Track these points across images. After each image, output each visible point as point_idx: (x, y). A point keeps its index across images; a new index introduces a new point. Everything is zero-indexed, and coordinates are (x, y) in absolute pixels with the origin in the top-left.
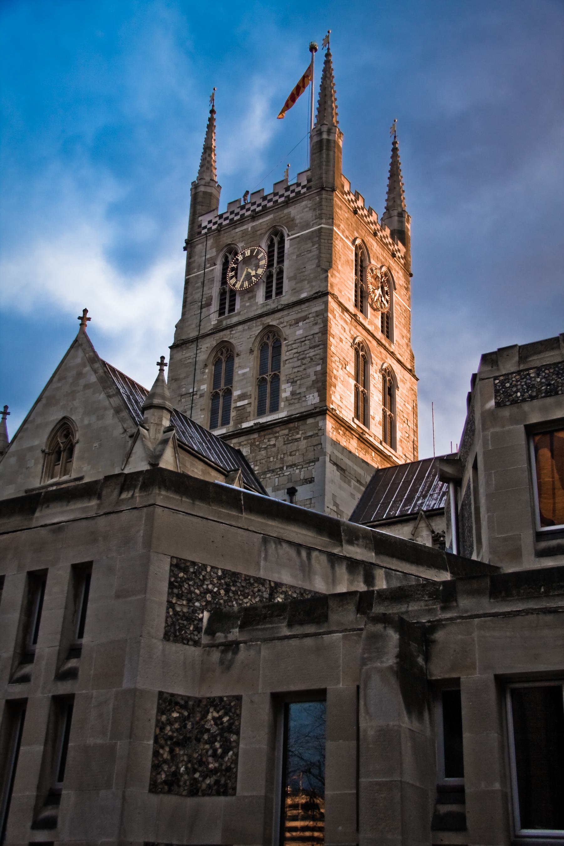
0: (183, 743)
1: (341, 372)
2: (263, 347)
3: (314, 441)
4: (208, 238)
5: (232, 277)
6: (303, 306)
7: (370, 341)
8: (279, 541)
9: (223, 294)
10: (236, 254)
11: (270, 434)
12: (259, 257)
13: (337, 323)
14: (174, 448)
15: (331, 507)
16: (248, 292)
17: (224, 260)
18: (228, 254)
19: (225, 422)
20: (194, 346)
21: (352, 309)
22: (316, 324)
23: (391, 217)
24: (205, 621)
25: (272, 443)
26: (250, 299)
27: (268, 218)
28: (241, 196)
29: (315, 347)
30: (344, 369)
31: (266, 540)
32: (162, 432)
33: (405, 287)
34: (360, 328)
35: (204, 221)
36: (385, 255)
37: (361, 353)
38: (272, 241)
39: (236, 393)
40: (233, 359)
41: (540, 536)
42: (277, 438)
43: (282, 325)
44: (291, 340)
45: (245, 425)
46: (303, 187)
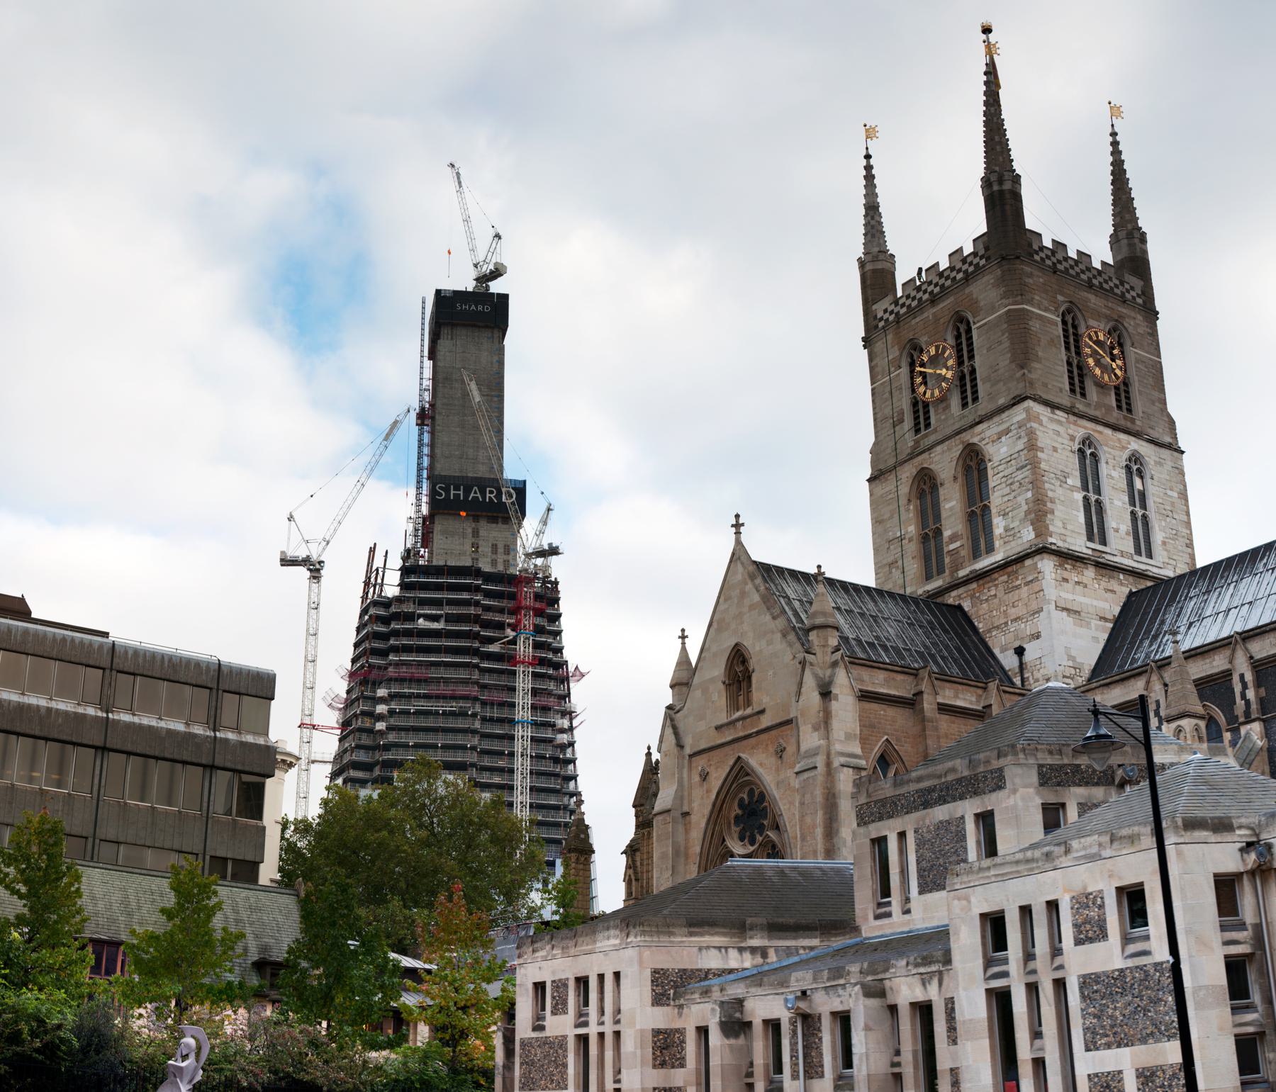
0: (667, 1048)
1: (1060, 491)
2: (967, 470)
3: (1035, 586)
4: (887, 332)
6: (1004, 415)
7: (1100, 433)
9: (915, 403)
10: (921, 351)
11: (989, 582)
12: (946, 355)
13: (1045, 430)
15: (1065, 663)
16: (942, 401)
17: (909, 360)
18: (912, 352)
19: (941, 571)
20: (892, 477)
21: (1065, 400)
22: (1020, 438)
24: (672, 995)
25: (993, 593)
27: (948, 301)
28: (915, 274)
29: (1022, 467)
30: (1065, 485)
31: (700, 949)
32: (830, 653)
33: (1148, 333)
35: (879, 308)
36: (1110, 304)
37: (1088, 452)
38: (958, 329)
39: (947, 533)
42: (996, 586)
43: (984, 442)
44: (996, 459)
45: (962, 573)
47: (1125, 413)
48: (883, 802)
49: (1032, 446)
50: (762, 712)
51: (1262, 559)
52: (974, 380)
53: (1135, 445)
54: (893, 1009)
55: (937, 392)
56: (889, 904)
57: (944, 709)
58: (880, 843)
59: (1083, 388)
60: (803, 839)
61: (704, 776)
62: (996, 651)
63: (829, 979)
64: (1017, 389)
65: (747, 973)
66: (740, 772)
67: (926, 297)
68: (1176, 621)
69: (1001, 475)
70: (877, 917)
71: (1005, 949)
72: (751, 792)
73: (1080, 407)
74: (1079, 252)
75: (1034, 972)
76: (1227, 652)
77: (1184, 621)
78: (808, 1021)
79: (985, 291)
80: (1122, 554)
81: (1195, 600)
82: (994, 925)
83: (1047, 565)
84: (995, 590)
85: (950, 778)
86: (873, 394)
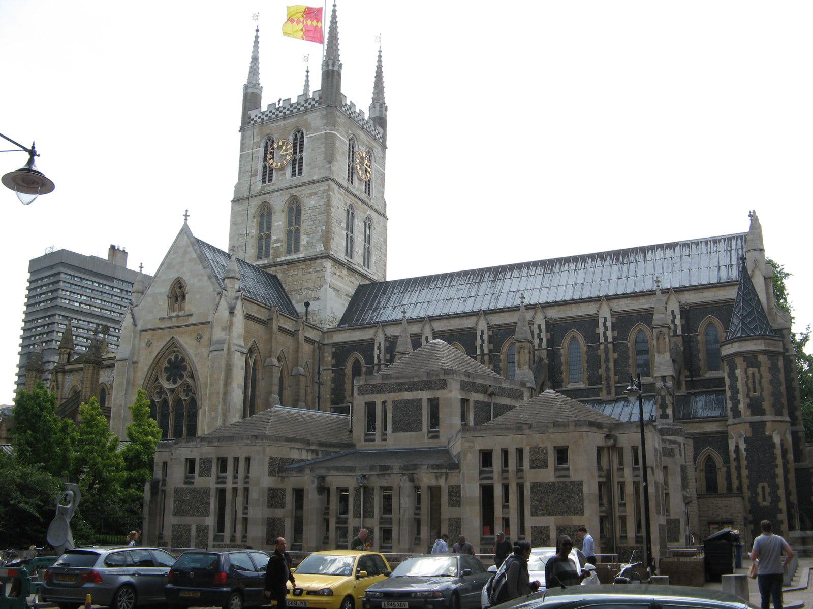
1: (337, 228)
2: (290, 209)
3: (321, 274)
5: (270, 159)
7: (357, 203)
8: (294, 448)
9: (265, 167)
10: (273, 142)
14: (242, 300)
19: (267, 256)
21: (345, 183)
22: (322, 198)
23: (374, 107)
26: (282, 174)
29: (322, 213)
31: (291, 448)
34: (350, 196)
35: (252, 113)
38: (296, 135)
39: (274, 238)
40: (271, 214)
41: (366, 435)
42: (298, 270)
44: (308, 206)
45: (279, 259)
46: (316, 102)
47: (367, 195)
48: (374, 386)
49: (328, 204)
50: (191, 315)
51: (433, 282)
52: (301, 163)
53: (370, 212)
54: (417, 488)
55: (279, 165)
56: (373, 435)
57: (281, 329)
58: (371, 407)
59: (352, 179)
60: (211, 385)
61: (149, 344)
62: (294, 302)
63: (380, 471)
64: (325, 174)
65: (310, 462)
66: (173, 345)
67: (281, 114)
68: (387, 304)
69: (309, 215)
70: (366, 441)
71: (491, 466)
72: (176, 357)
73: (351, 189)
74: (360, 110)
75: (507, 478)
76: (420, 325)
77: (391, 304)
78: (366, 490)
79: (315, 119)
80: (358, 265)
81: (397, 295)
82: (486, 457)
83: (328, 264)
84: (297, 273)
85: (415, 379)
86: (241, 157)
